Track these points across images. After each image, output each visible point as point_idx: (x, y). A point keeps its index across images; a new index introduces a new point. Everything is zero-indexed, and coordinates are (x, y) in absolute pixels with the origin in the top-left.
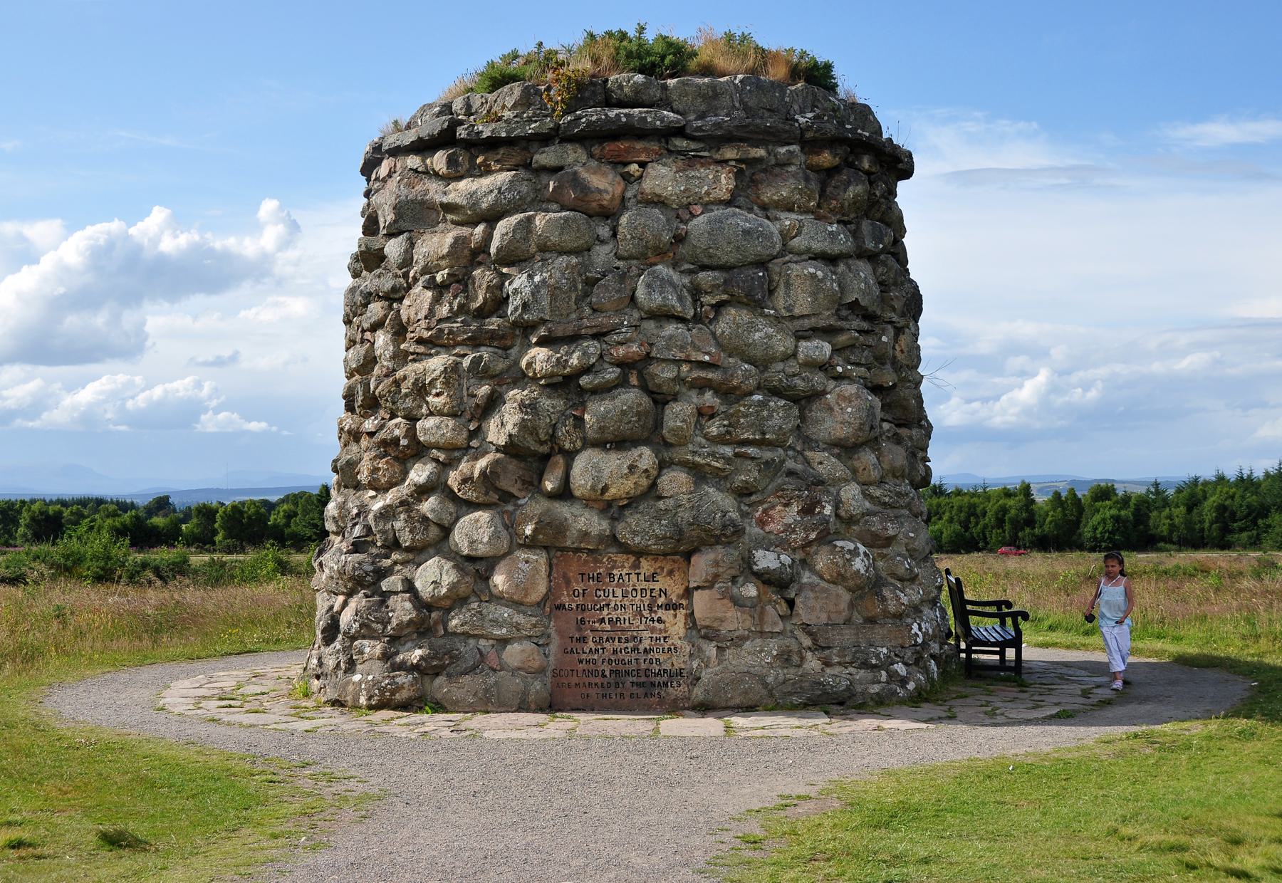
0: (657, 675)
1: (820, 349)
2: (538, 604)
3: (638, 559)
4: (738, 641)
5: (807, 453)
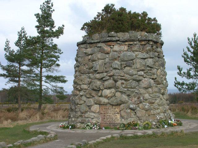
1: (142, 73)
4: (127, 119)
5: (140, 89)
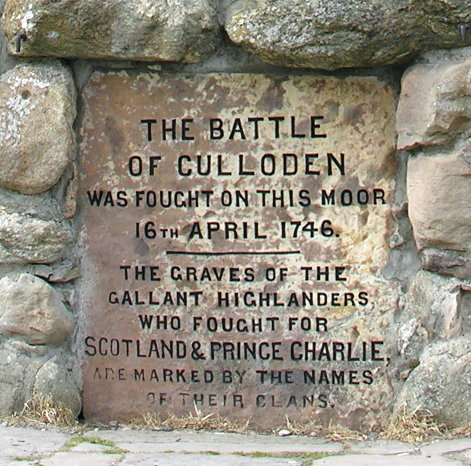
0: (317, 355)
2: (50, 190)
3: (277, 83)
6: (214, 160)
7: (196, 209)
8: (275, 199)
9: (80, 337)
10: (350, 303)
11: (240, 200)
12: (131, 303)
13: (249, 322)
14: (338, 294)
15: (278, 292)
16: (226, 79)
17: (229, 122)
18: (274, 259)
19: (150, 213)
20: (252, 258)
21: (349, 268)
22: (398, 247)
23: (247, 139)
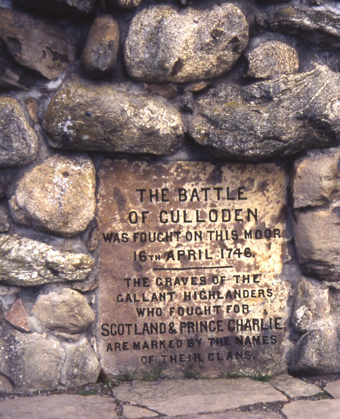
6: (181, 213)
7: (171, 243)
8: (217, 236)
9: (99, 325)
10: (262, 296)
11: (197, 237)
12: (131, 301)
13: (203, 309)
14: (255, 291)
15: (220, 290)
16: (187, 165)
17: (190, 190)
18: (217, 271)
19: (143, 246)
20: (204, 271)
21: (261, 275)
22: (287, 263)
23: (201, 201)
